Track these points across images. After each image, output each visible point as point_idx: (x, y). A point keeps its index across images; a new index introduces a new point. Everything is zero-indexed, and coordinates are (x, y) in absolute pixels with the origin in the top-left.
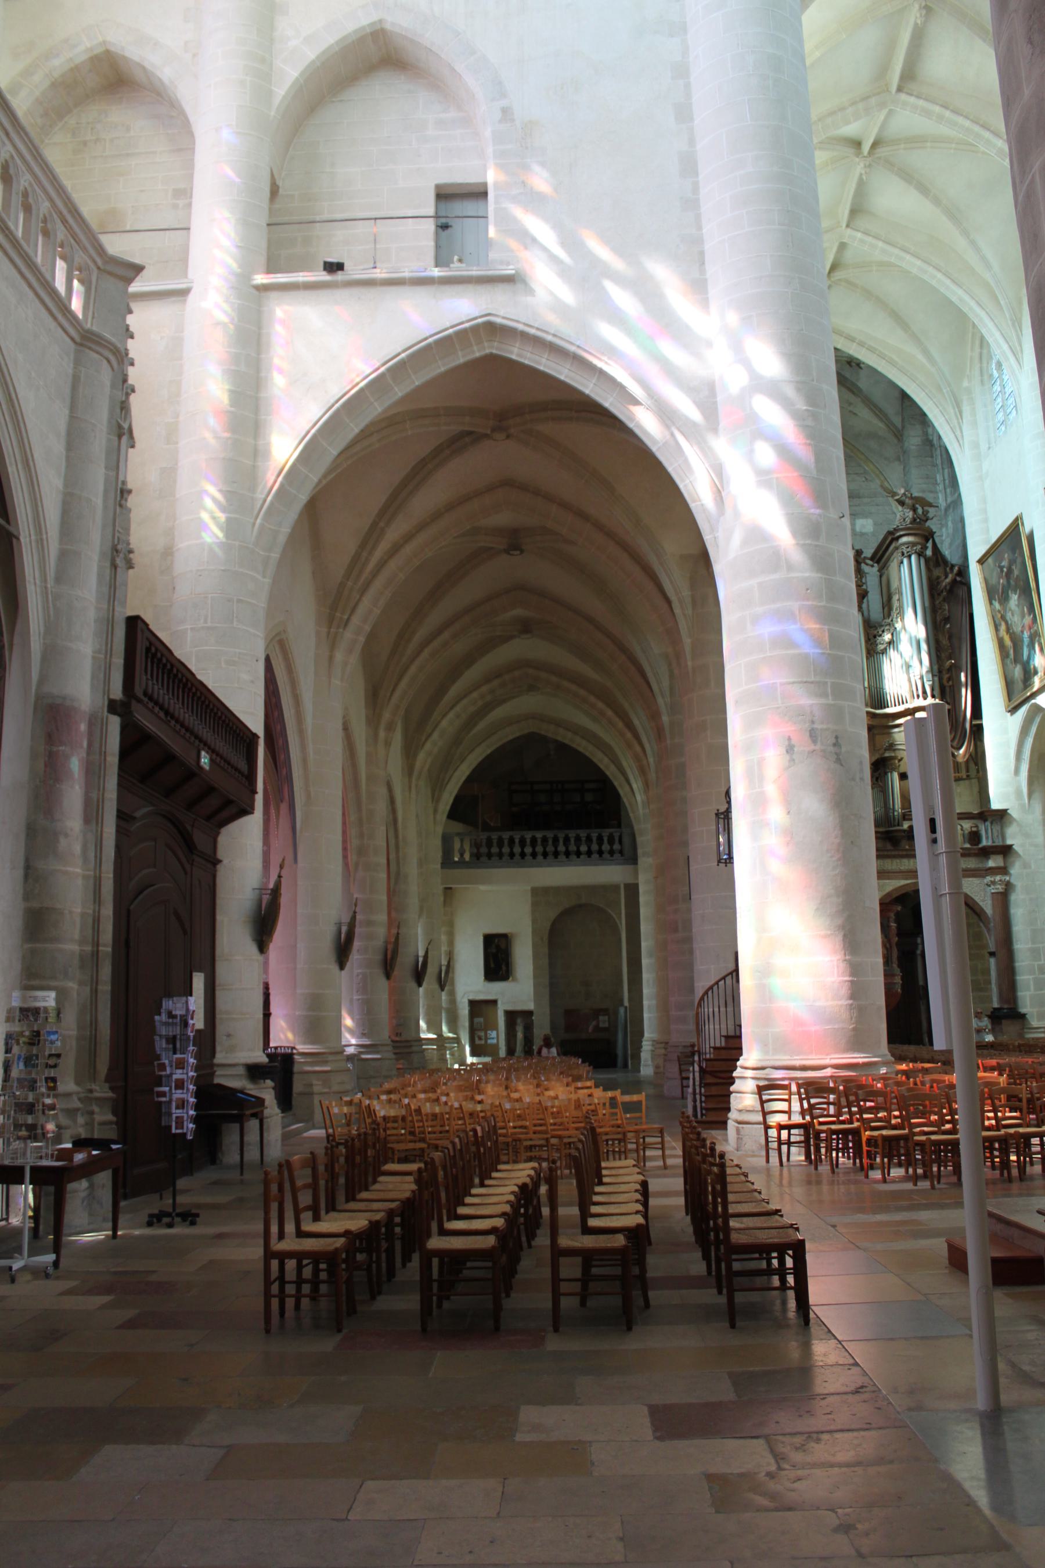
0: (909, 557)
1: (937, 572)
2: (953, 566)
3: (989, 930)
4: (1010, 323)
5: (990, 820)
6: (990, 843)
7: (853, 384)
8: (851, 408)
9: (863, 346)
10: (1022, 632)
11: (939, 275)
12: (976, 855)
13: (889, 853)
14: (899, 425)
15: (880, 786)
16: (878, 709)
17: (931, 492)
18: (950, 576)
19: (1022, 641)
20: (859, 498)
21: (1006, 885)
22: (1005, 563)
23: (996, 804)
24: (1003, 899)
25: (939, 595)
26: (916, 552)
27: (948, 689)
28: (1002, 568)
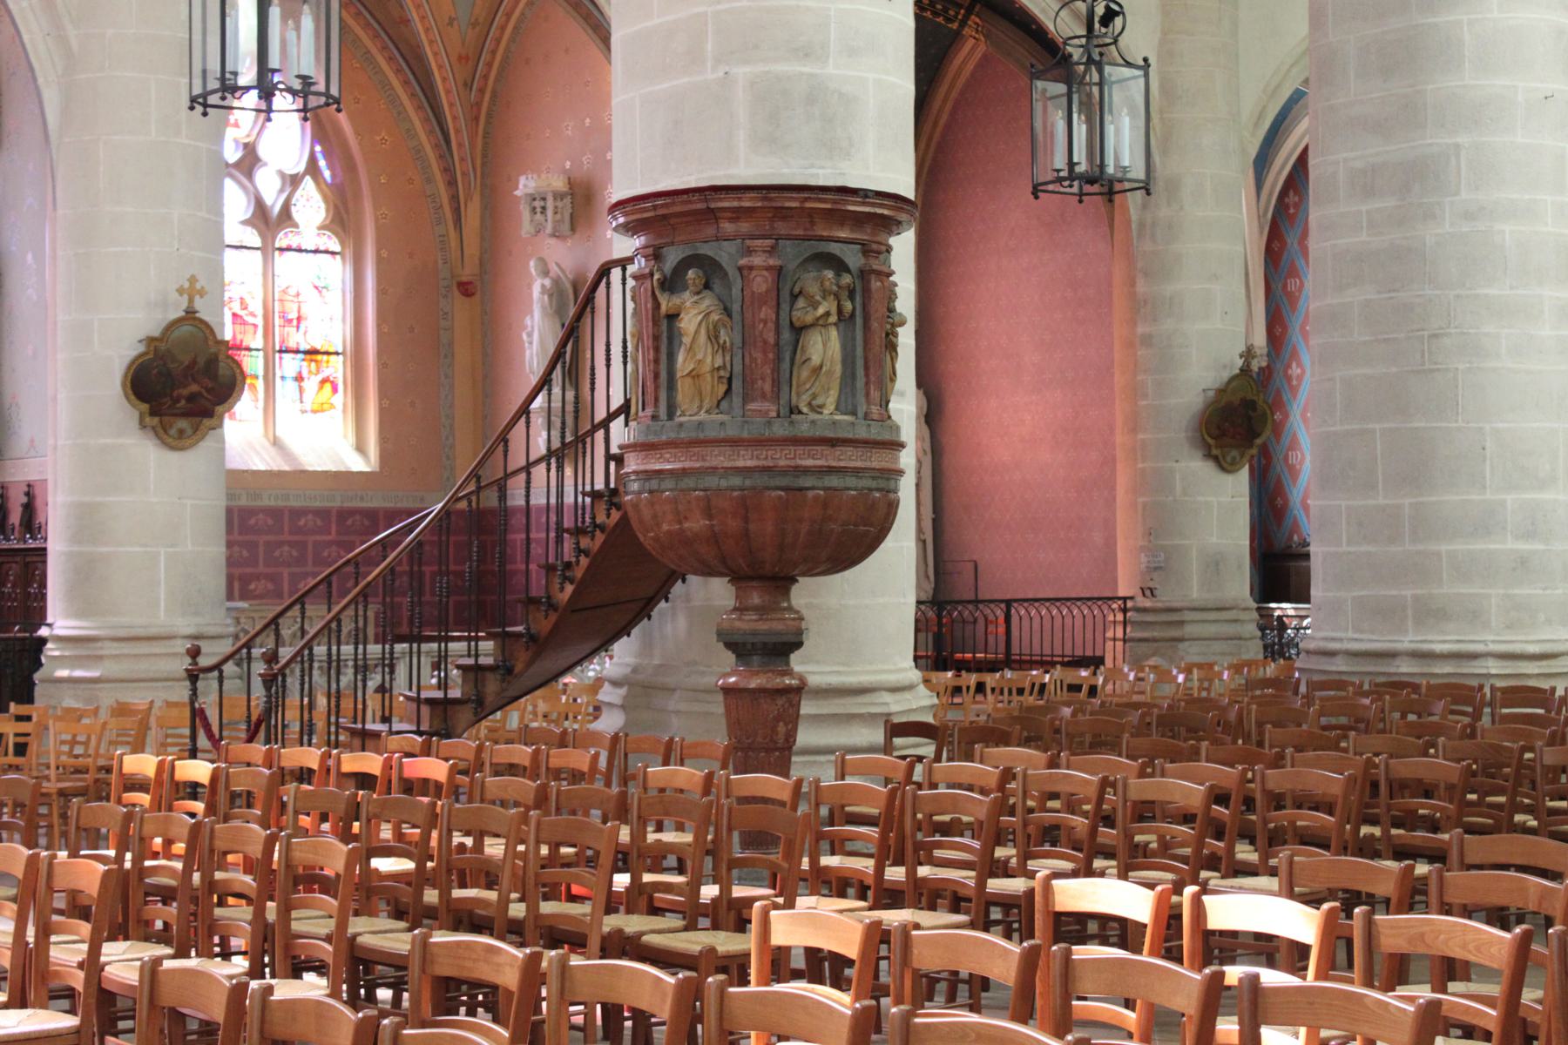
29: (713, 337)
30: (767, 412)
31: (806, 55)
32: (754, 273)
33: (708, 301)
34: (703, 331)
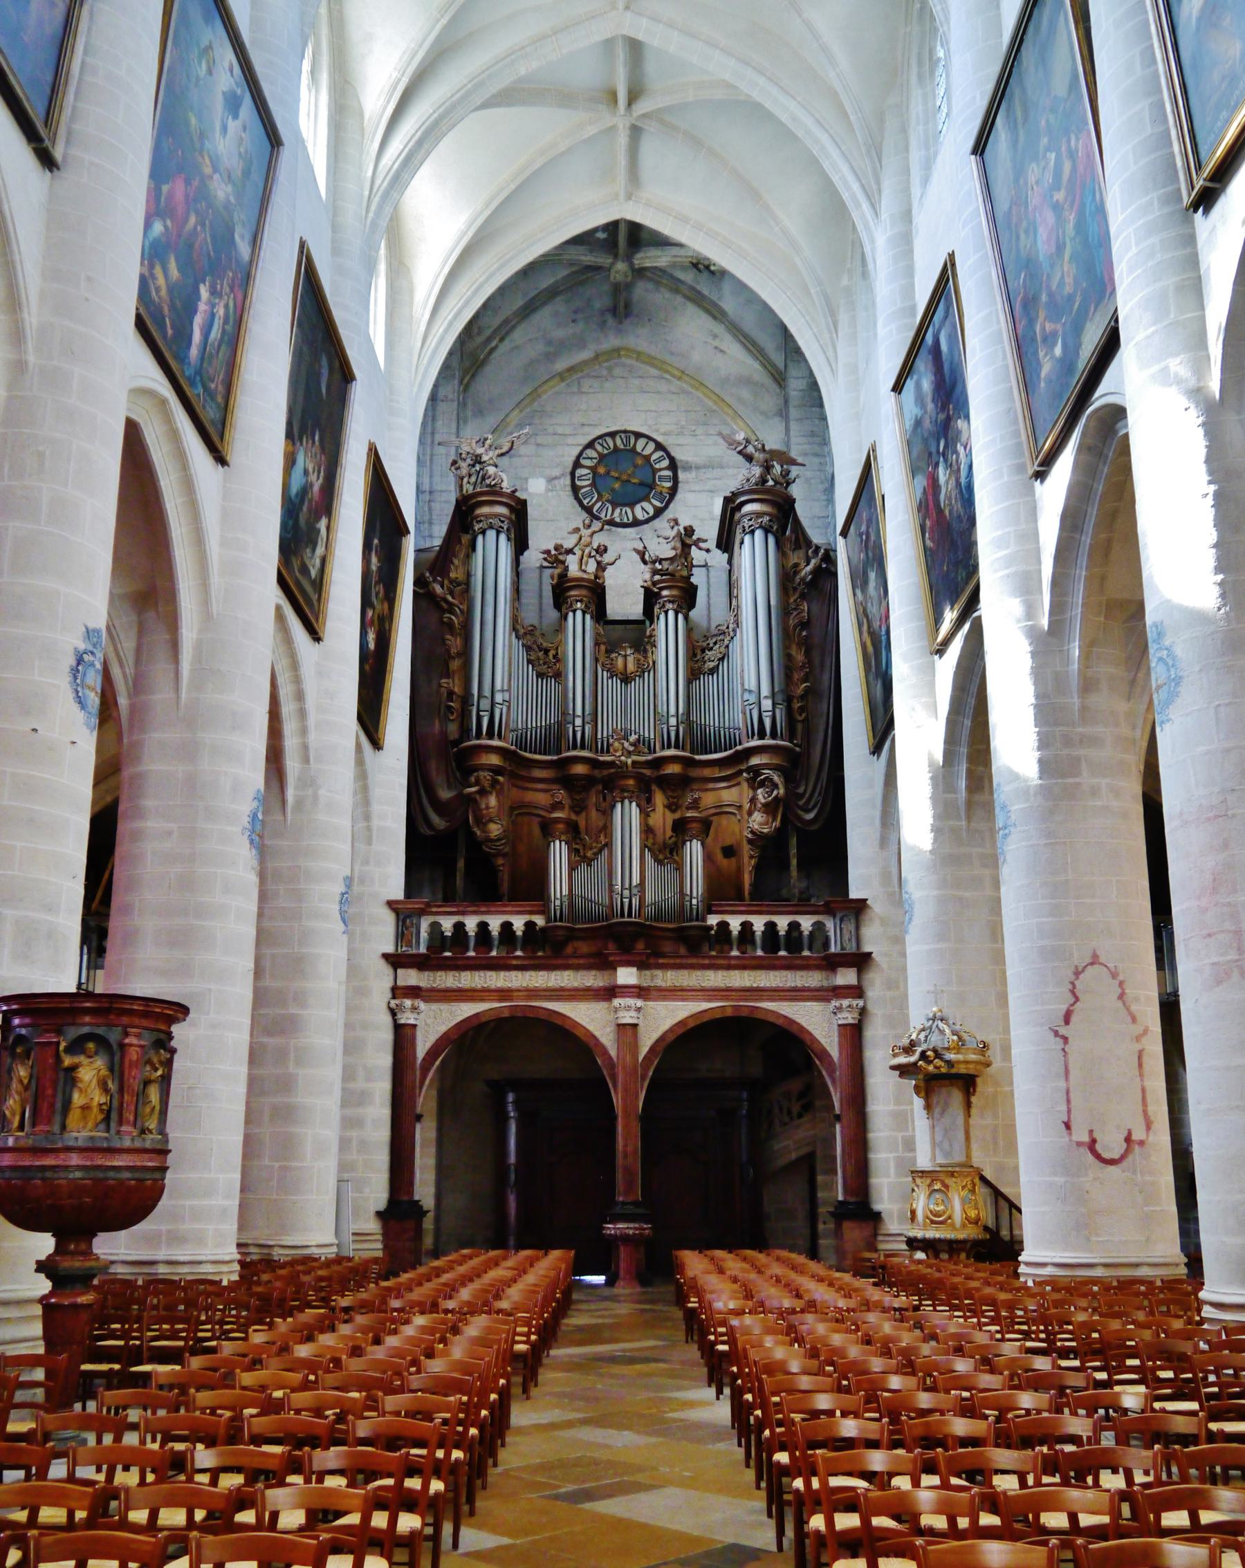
0: (752, 532)
1: (795, 558)
2: (818, 548)
3: (834, 1082)
4: (863, 150)
5: (839, 916)
6: (838, 950)
7: (715, 305)
8: (716, 343)
9: (701, 230)
10: (880, 627)
11: (761, 81)
12: (818, 967)
13: (684, 961)
14: (781, 365)
15: (676, 862)
16: (702, 754)
17: (816, 455)
18: (813, 562)
19: (881, 641)
20: (722, 467)
21: (860, 1014)
22: (863, 528)
23: (854, 894)
24: (854, 1035)
25: (795, 589)
26: (761, 527)
27: (799, 727)
28: (861, 535)
29: (103, 1086)
30: (131, 1132)
31: (50, 910)
32: (132, 1048)
33: (100, 1063)
34: (95, 1082)
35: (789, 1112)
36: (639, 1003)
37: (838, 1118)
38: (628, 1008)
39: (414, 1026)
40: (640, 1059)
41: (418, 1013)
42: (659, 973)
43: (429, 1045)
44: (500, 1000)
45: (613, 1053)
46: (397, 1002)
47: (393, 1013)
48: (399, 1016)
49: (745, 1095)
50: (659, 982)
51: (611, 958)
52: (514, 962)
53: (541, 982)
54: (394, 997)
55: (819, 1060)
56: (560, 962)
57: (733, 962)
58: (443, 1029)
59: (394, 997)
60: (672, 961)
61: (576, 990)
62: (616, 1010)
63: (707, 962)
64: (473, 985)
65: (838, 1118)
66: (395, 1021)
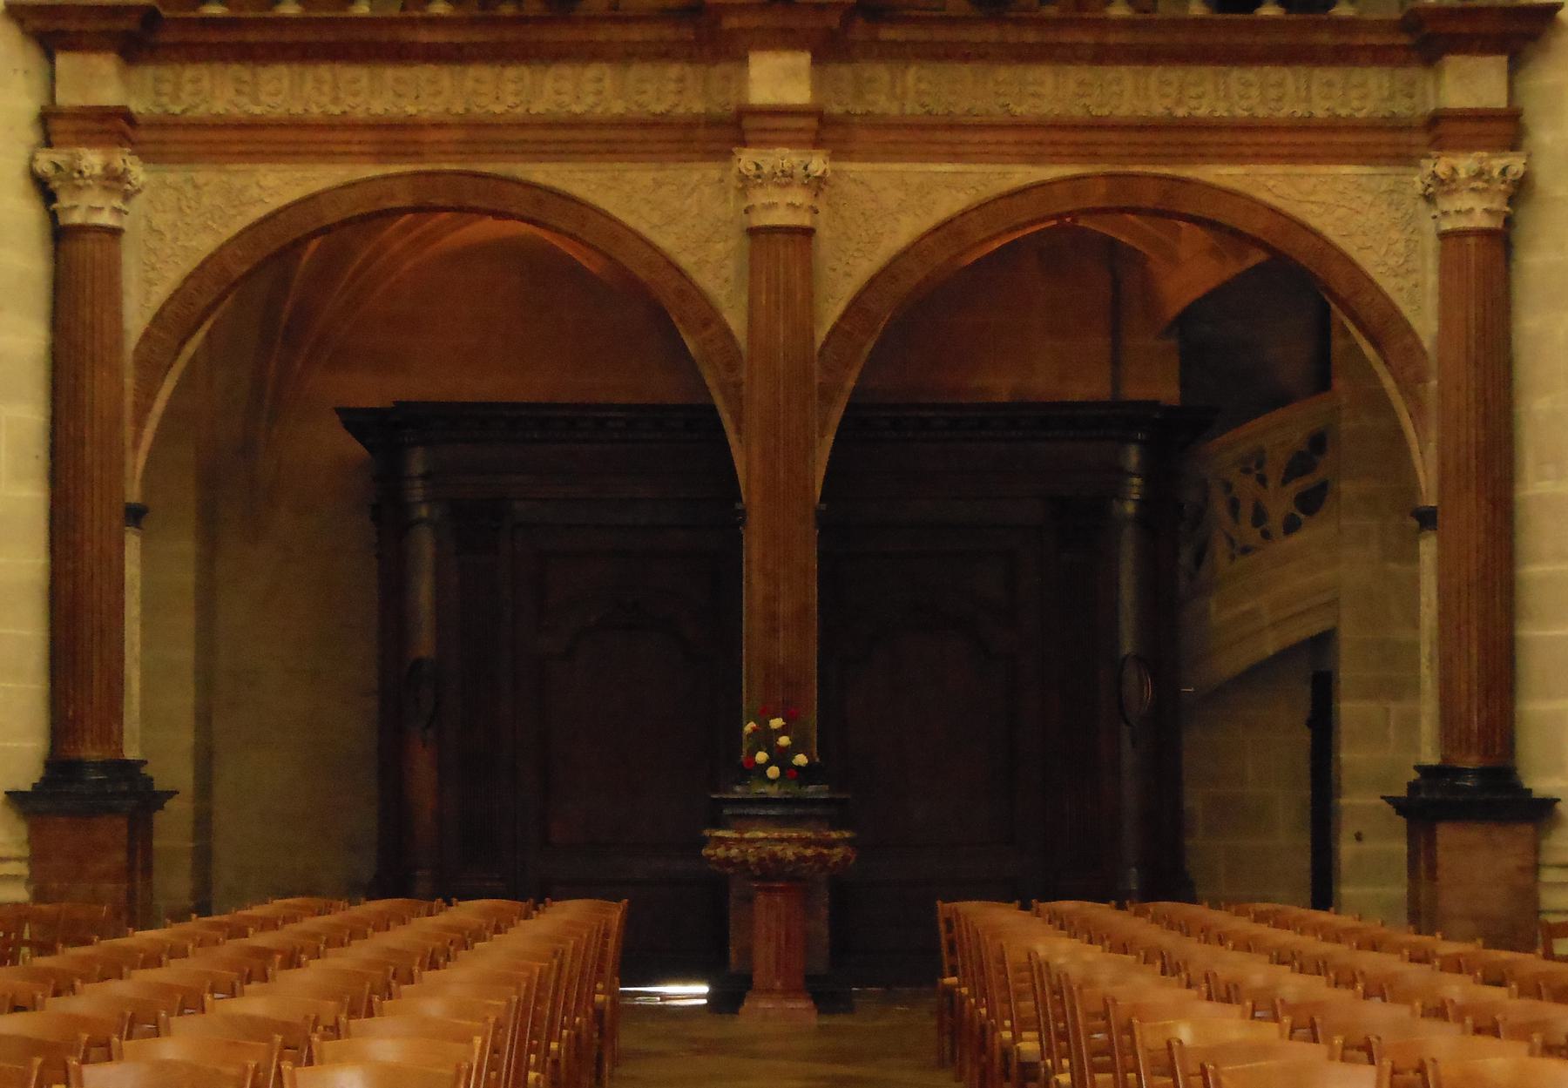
3: (1418, 412)
35: (1259, 517)
36: (818, 164)
37: (1427, 519)
38: (785, 179)
39: (115, 232)
40: (821, 335)
41: (127, 197)
42: (881, 73)
43: (161, 293)
44: (381, 156)
45: (736, 321)
46: (60, 156)
47: (45, 190)
48: (64, 201)
49: (1132, 457)
50: (883, 104)
51: (732, 22)
52: (424, 36)
53: (511, 100)
54: (48, 143)
55: (1376, 344)
56: (566, 34)
57: (1112, 39)
58: (206, 244)
59: (48, 143)
60: (920, 35)
61: (621, 123)
62: (746, 183)
63: (1031, 36)
64: (297, 109)
65: (1427, 519)
66: (53, 216)
